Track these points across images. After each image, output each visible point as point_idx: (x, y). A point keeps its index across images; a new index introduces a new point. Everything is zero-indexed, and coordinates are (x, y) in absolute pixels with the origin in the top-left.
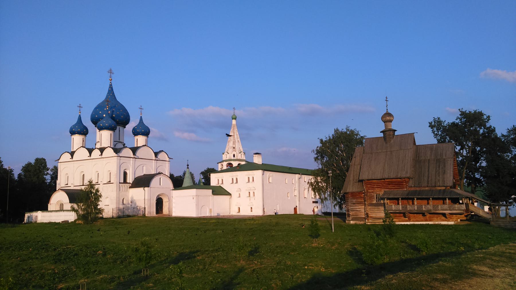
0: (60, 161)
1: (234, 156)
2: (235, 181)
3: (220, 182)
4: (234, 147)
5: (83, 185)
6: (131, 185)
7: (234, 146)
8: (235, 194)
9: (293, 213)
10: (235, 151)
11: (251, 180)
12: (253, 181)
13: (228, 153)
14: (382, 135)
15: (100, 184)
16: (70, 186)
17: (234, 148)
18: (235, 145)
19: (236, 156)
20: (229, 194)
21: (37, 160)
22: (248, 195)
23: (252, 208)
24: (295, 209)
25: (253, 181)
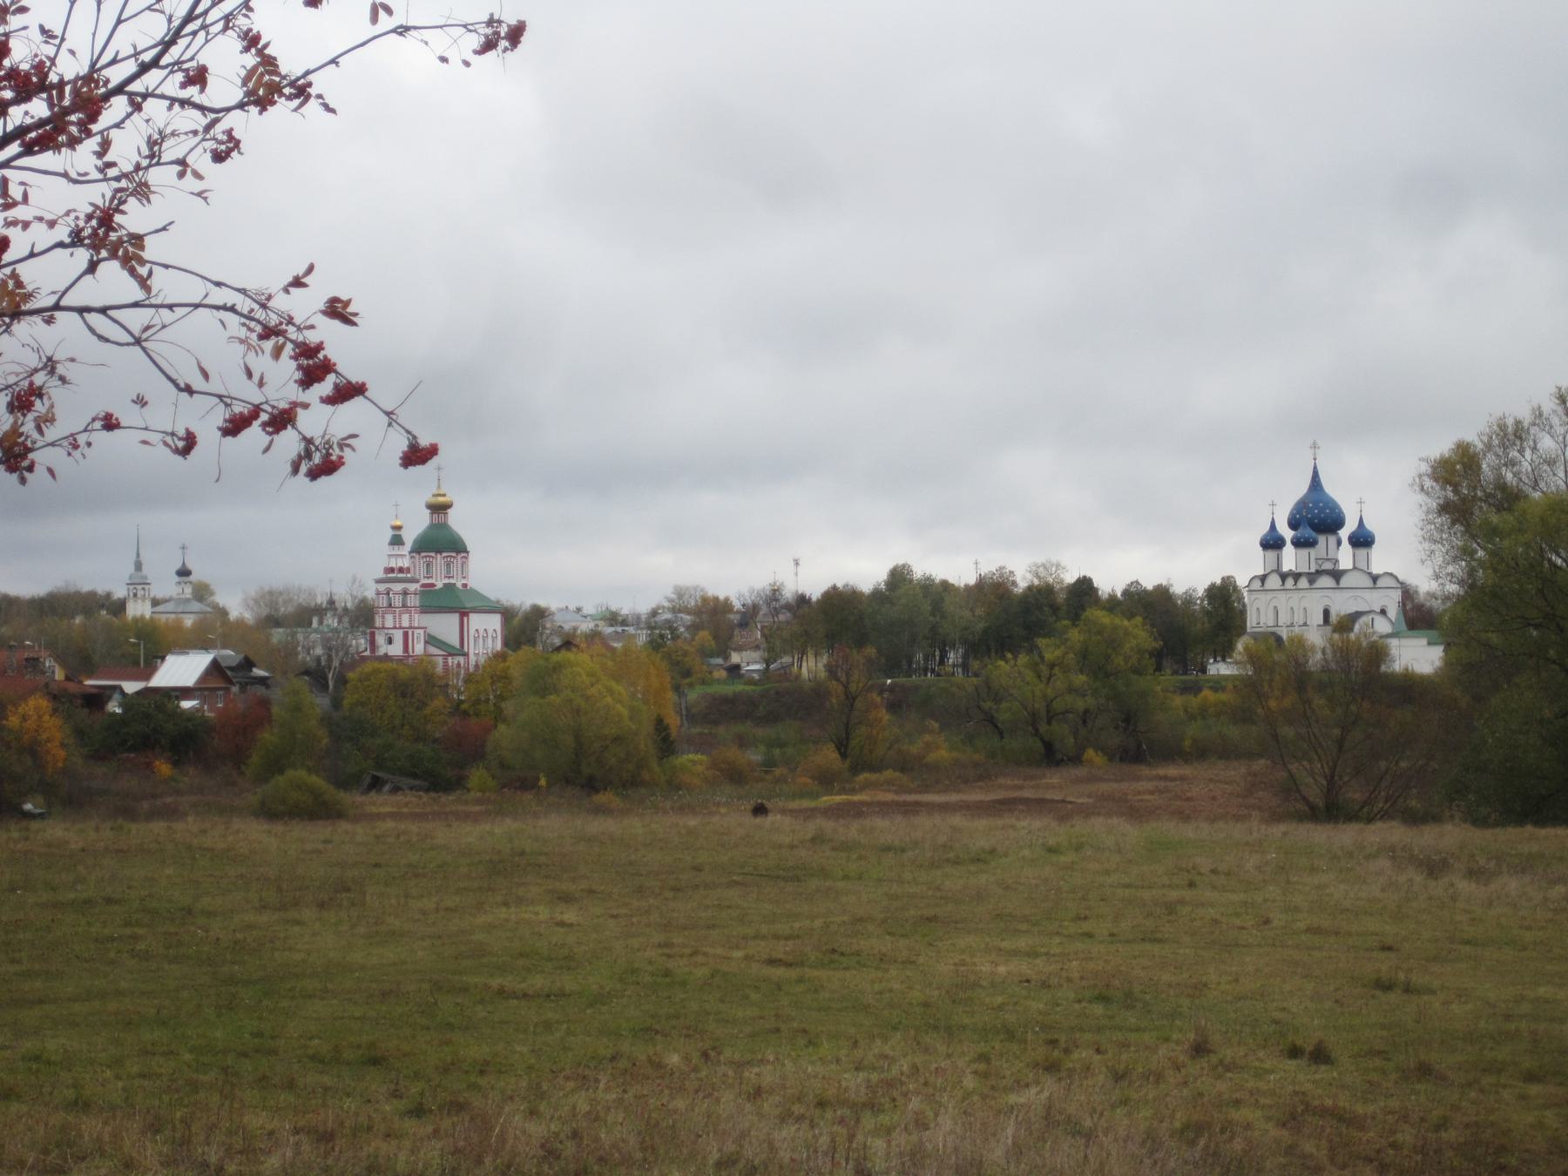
5: (1277, 626)
21: (1223, 578)
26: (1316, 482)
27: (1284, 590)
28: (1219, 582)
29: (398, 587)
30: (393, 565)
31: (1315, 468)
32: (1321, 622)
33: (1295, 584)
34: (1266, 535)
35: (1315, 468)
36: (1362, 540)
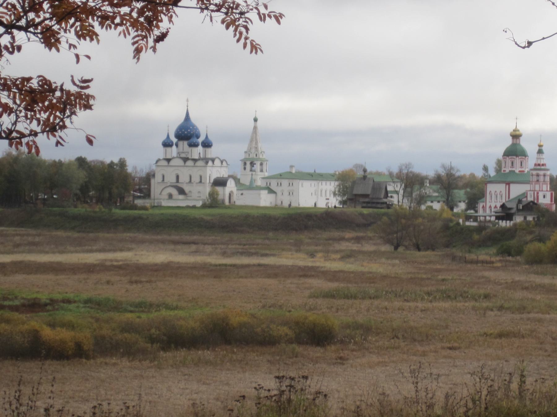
3: (268, 184)
7: (256, 146)
8: (279, 194)
9: (314, 206)
11: (291, 184)
13: (251, 153)
19: (258, 156)
22: (288, 194)
24: (315, 204)
29: (541, 173)
30: (539, 162)
36: (207, 144)
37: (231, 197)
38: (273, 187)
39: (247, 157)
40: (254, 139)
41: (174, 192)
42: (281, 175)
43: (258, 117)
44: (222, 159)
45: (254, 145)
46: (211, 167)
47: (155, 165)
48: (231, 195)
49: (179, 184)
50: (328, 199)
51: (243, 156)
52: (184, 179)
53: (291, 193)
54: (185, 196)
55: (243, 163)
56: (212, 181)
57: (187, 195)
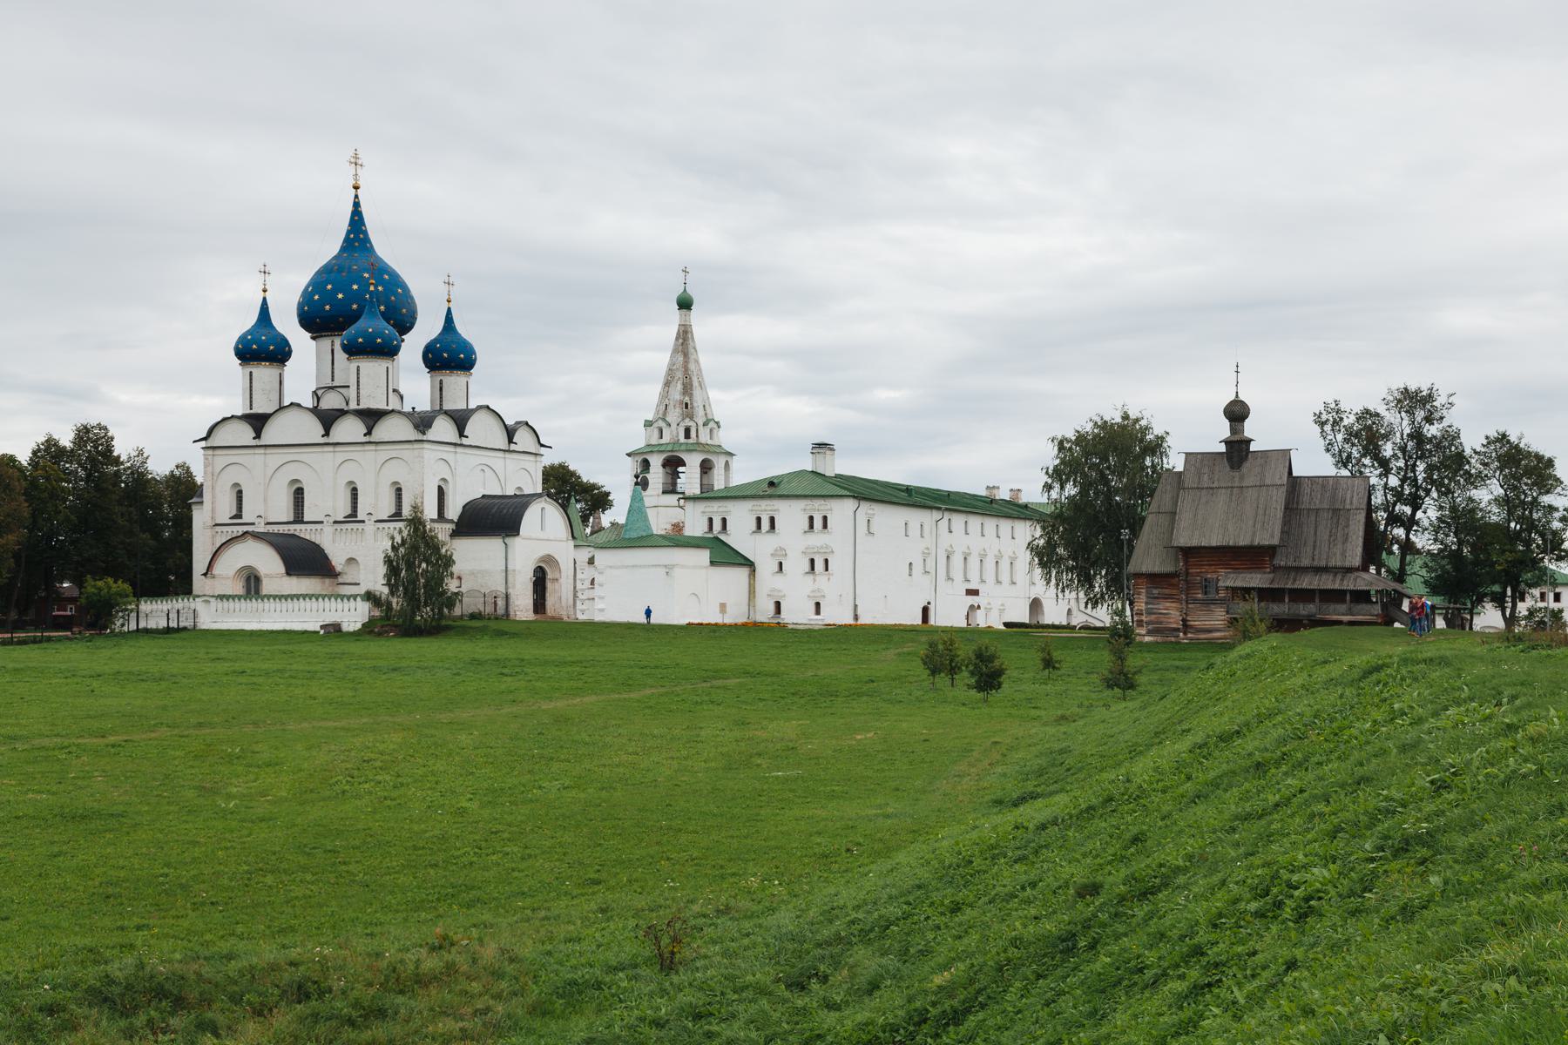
0: (212, 442)
1: (687, 435)
2: (765, 525)
3: (717, 526)
4: (687, 404)
5: (302, 522)
6: (452, 526)
7: (687, 399)
8: (765, 567)
10: (692, 419)
11: (818, 523)
12: (825, 526)
14: (1222, 448)
15: (363, 522)
16: (253, 524)
17: (687, 407)
18: (691, 395)
19: (693, 434)
20: (749, 564)
21: (83, 434)
22: (807, 567)
23: (818, 604)
25: (825, 526)
26: (356, 239)
27: (370, 443)
28: (66, 440)
31: (356, 205)
32: (436, 517)
33: (369, 433)
34: (248, 332)
35: (356, 205)
37: (549, 585)
38: (740, 537)
39: (655, 440)
40: (679, 374)
41: (268, 562)
42: (772, 484)
43: (692, 292)
44: (510, 422)
45: (676, 393)
46: (451, 449)
47: (203, 444)
48: (550, 576)
49: (303, 527)
50: (973, 592)
51: (639, 439)
52: (325, 502)
53: (819, 565)
54: (327, 581)
55: (640, 459)
56: (453, 512)
57: (340, 580)
